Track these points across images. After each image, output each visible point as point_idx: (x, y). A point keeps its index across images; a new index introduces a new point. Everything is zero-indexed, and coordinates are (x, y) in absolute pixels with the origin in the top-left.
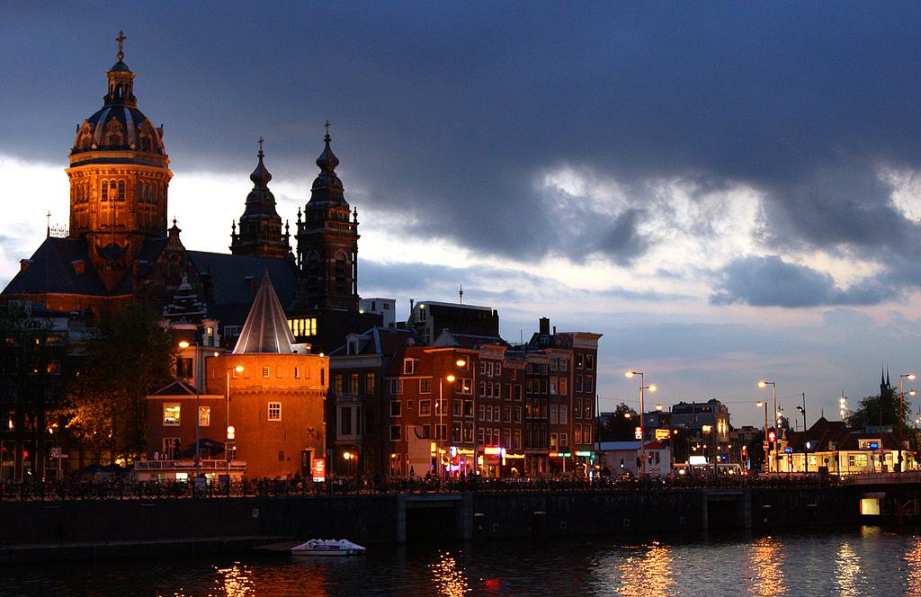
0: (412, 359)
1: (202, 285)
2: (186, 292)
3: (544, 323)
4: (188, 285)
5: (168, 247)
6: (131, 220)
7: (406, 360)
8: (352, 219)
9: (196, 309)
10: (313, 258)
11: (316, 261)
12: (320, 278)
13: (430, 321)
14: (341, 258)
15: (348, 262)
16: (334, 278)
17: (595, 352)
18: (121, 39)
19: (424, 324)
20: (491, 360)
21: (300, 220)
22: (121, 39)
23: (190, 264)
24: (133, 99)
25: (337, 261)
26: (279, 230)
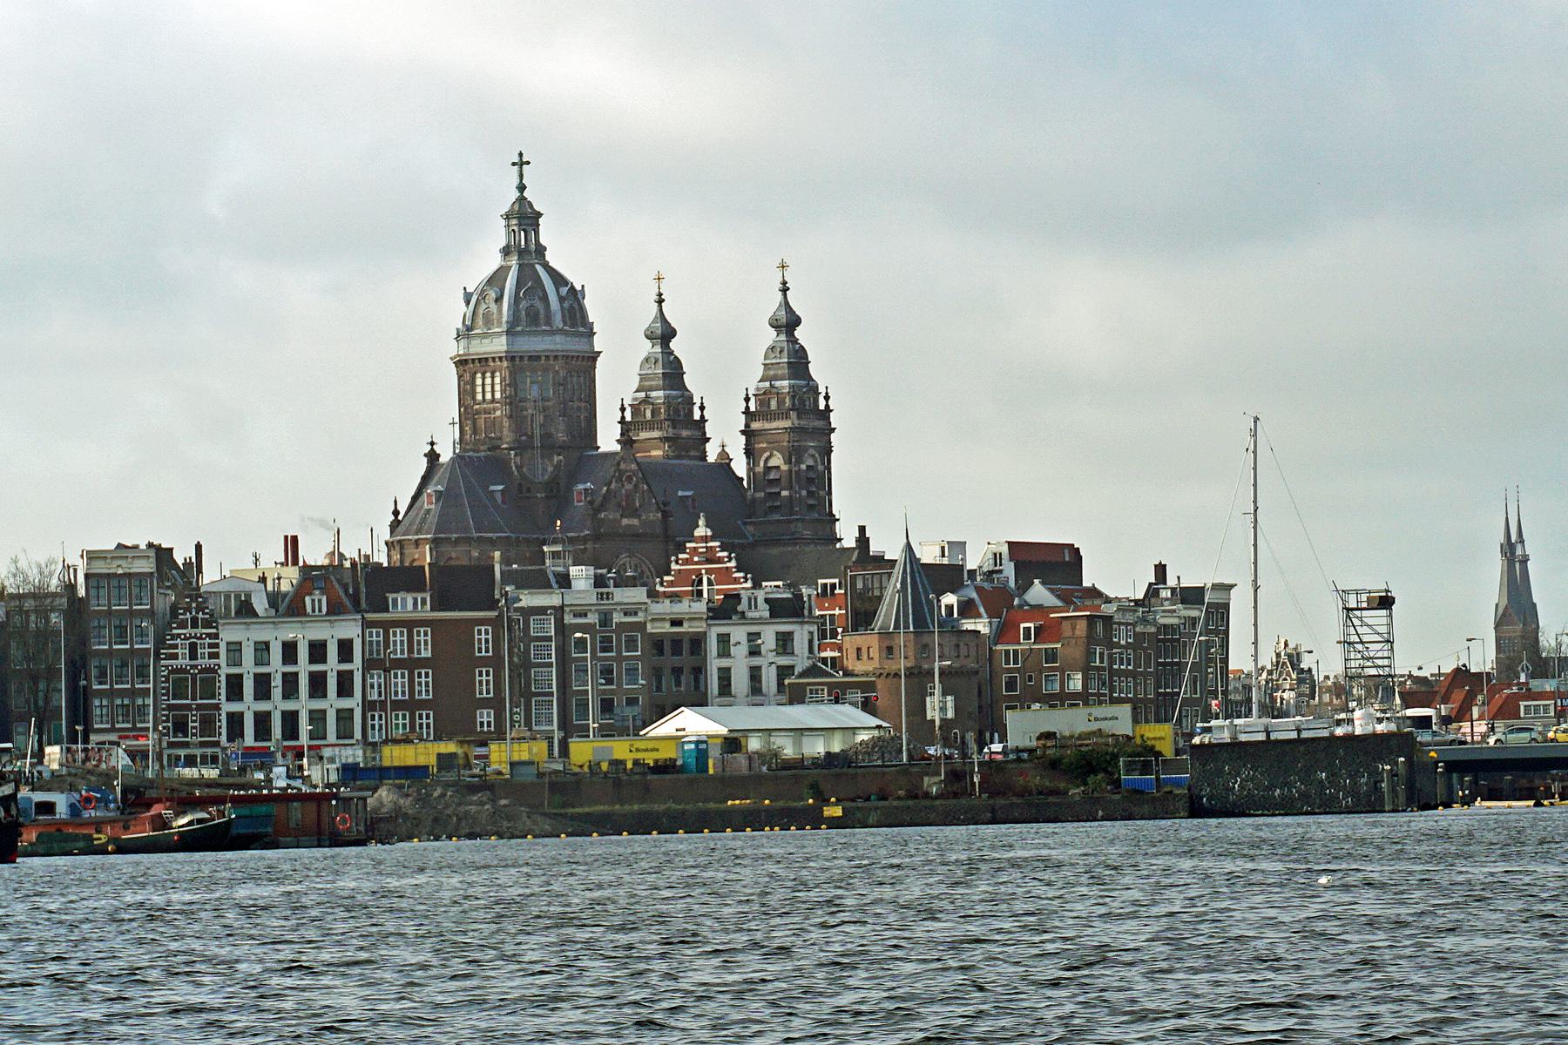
0: (1031, 625)
1: (660, 515)
2: (705, 539)
3: (1161, 570)
4: (708, 530)
5: (623, 466)
6: (562, 427)
7: (1022, 625)
8: (822, 406)
9: (720, 560)
10: (772, 463)
11: (778, 467)
12: (785, 493)
13: (1009, 569)
14: (810, 462)
15: (820, 468)
16: (804, 493)
17: (1226, 606)
18: (521, 163)
19: (1000, 571)
20: (1123, 624)
21: (747, 408)
22: (521, 163)
23: (645, 487)
24: (541, 250)
25: (807, 466)
26: (691, 412)
